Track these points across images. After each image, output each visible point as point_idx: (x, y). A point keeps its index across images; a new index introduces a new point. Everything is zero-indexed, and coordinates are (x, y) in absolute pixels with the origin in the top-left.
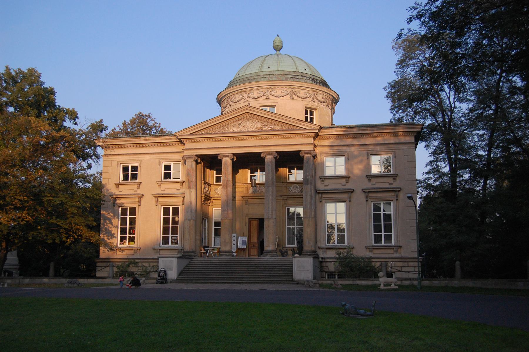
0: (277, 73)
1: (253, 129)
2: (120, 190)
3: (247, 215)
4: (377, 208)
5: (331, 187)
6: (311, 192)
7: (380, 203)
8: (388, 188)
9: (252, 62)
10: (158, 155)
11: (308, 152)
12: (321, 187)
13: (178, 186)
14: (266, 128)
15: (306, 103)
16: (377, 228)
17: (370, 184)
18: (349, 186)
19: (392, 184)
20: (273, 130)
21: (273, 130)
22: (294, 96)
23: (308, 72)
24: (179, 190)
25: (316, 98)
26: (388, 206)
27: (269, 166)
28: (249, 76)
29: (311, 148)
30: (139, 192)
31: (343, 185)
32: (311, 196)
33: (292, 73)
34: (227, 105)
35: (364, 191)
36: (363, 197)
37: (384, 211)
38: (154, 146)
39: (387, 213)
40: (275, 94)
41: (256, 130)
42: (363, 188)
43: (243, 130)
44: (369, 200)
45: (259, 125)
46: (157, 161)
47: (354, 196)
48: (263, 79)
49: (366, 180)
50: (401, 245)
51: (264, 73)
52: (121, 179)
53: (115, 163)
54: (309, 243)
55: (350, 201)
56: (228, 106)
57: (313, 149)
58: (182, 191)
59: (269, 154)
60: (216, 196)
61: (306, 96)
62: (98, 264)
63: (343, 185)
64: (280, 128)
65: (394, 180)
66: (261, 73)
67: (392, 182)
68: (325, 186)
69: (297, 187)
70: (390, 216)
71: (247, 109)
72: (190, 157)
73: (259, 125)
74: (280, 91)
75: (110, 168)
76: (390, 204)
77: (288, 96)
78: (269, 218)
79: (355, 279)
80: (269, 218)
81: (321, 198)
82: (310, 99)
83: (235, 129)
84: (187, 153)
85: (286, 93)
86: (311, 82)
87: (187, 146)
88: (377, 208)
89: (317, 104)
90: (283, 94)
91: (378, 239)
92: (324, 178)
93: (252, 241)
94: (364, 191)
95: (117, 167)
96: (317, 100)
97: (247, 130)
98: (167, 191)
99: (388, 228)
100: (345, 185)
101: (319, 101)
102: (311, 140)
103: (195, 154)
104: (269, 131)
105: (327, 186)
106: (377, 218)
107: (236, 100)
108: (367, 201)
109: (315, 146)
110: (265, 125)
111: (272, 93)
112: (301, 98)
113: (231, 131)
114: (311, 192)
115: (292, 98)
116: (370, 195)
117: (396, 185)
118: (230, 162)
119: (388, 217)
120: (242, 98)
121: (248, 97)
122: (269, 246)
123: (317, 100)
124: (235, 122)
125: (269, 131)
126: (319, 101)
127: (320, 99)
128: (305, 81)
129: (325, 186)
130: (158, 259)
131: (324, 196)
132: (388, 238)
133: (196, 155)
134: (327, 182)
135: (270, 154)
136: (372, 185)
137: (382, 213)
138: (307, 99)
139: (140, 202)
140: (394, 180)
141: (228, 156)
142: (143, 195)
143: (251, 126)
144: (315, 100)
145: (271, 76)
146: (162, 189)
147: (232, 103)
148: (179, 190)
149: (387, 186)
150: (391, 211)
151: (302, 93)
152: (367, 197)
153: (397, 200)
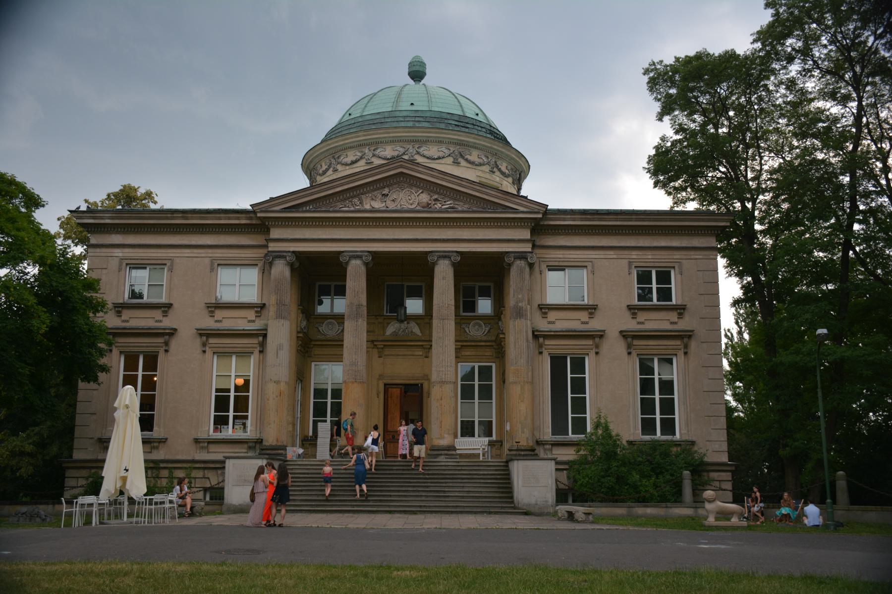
0: (428, 114)
1: (413, 207)
2: (123, 318)
3: (381, 377)
4: (646, 369)
5: (560, 326)
6: (527, 332)
7: (653, 359)
8: (671, 331)
9: (375, 94)
10: (210, 251)
11: (522, 256)
12: (543, 325)
14: (438, 206)
15: (480, 174)
16: (647, 406)
17: (634, 322)
18: (595, 324)
19: (676, 323)
20: (453, 209)
21: (453, 209)
22: (460, 160)
23: (481, 118)
24: (253, 321)
25: (497, 166)
26: (668, 365)
27: (444, 278)
28: (373, 117)
29: (527, 247)
30: (167, 323)
31: (583, 323)
32: (528, 341)
33: (456, 118)
34: (327, 170)
35: (624, 335)
36: (620, 347)
37: (659, 375)
38: (203, 233)
39: (665, 377)
40: (426, 153)
41: (418, 208)
42: (624, 328)
43: (392, 206)
44: (634, 353)
46: (207, 261)
47: (605, 346)
48: (403, 124)
49: (628, 314)
50: (694, 439)
51: (405, 114)
52: (126, 296)
53: (114, 263)
54: (523, 432)
55: (597, 353)
56: (330, 172)
57: (530, 250)
58: (258, 325)
59: (445, 257)
60: (320, 337)
61: (481, 161)
62: (69, 473)
63: (583, 323)
64: (466, 207)
65: (681, 316)
66: (398, 114)
67: (676, 320)
68: (549, 323)
69: (480, 326)
70: (671, 383)
71: (401, 167)
72: (279, 255)
73: (424, 198)
74: (436, 148)
75: (104, 271)
76: (670, 362)
77: (450, 160)
78: (443, 383)
79: (669, 504)
80: (443, 383)
81: (541, 346)
82: (487, 168)
83: (377, 205)
84: (273, 247)
85: (447, 152)
86: (489, 136)
87: (275, 233)
89: (498, 179)
90: (441, 154)
92: (545, 309)
93: (389, 429)
94: (624, 335)
95: (120, 270)
96: (500, 170)
97: (399, 207)
98: (227, 325)
99: (668, 406)
100: (587, 323)
101: (503, 173)
102: (526, 234)
103: (292, 249)
104: (446, 211)
105: (553, 323)
106: (646, 386)
107: (349, 160)
108: (629, 353)
109: (534, 246)
110: (436, 200)
111: (421, 150)
112: (472, 163)
113: (368, 207)
114: (527, 332)
115: (456, 163)
116: (636, 342)
117: (684, 324)
118: (363, 269)
119: (667, 387)
120: (361, 158)
121: (374, 155)
122: (443, 438)
123: (500, 170)
124: (375, 190)
125: (446, 211)
126: (503, 173)
127: (503, 169)
128: (481, 133)
129: (549, 323)
130: (224, 462)
131: (547, 342)
133: (293, 252)
134: (552, 316)
135: (445, 255)
136: (639, 323)
137: (656, 377)
138: (484, 168)
139: (167, 344)
140: (681, 316)
141: (360, 257)
142: (175, 330)
143: (407, 200)
144: (495, 170)
145: (417, 119)
146: (216, 318)
147: (339, 167)
148: (253, 321)
149: (666, 326)
150: (675, 375)
151: (474, 156)
152: (629, 346)
153: (686, 353)
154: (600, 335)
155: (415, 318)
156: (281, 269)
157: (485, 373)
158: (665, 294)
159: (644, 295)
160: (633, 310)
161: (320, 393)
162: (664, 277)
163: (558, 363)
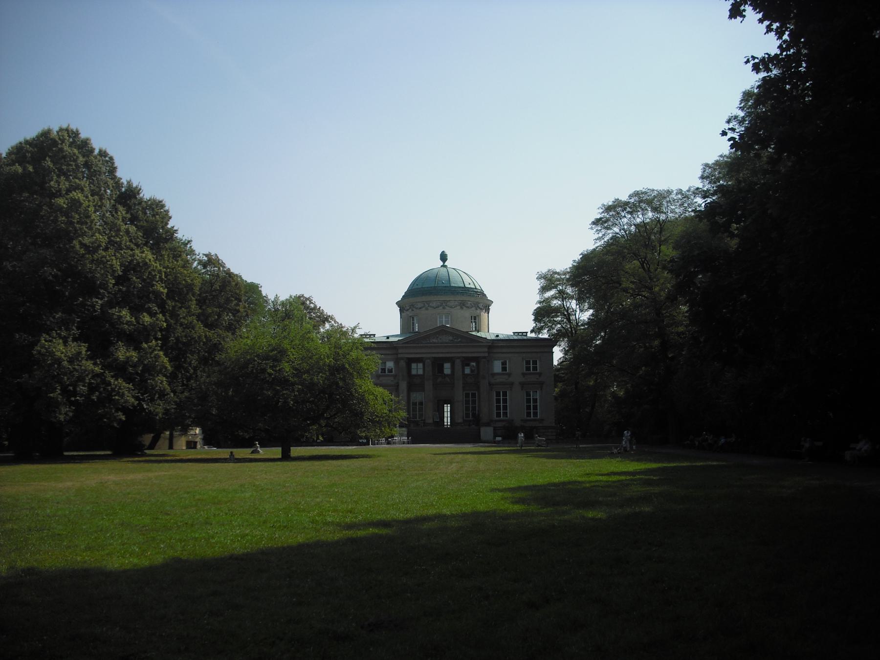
4: (528, 394)
13: (392, 379)
16: (529, 407)
29: (486, 355)
45: (451, 338)
72: (402, 359)
73: (451, 338)
84: (399, 356)
87: (400, 351)
88: (528, 394)
91: (529, 414)
102: (486, 350)
106: (528, 401)
119: (535, 400)
132: (535, 414)
135: (459, 358)
154: (512, 384)
155: (448, 375)
156: (403, 364)
157: (474, 395)
158: (535, 368)
159: (528, 369)
160: (524, 374)
161: (414, 404)
162: (535, 363)
163: (498, 394)
